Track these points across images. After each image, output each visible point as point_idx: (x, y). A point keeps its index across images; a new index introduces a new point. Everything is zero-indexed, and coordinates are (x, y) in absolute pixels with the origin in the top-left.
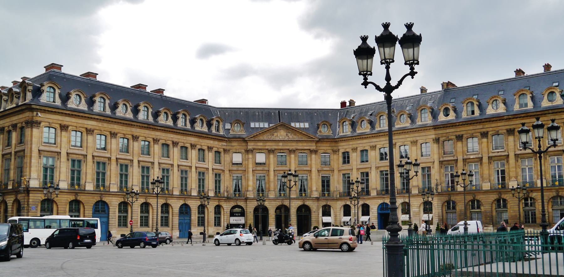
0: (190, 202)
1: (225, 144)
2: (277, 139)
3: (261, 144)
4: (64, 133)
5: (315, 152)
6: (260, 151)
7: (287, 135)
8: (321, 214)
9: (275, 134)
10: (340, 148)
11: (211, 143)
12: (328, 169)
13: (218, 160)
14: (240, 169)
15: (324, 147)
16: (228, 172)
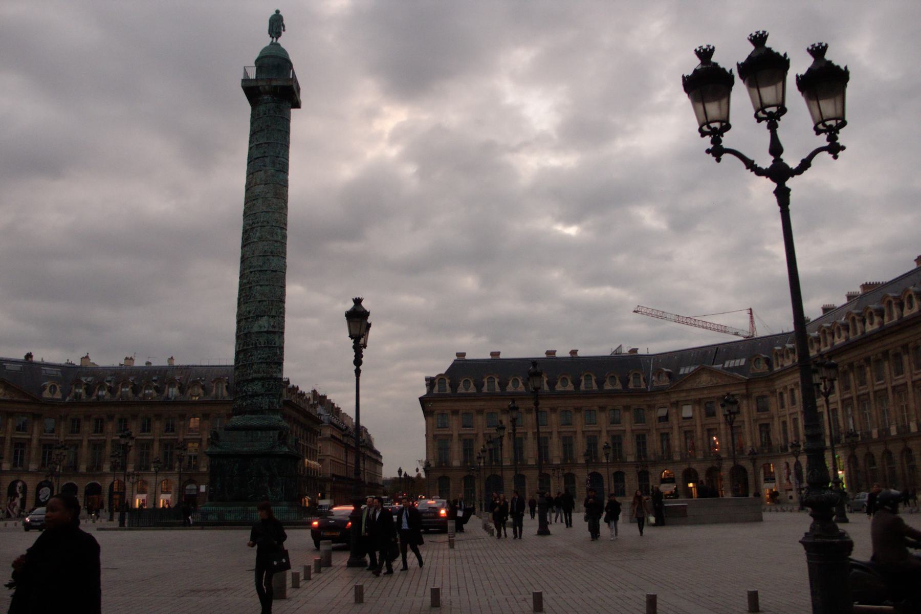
0: (602, 471)
1: (648, 399)
2: (701, 386)
3: (684, 394)
4: (454, 418)
5: (747, 396)
6: (686, 403)
7: (711, 379)
8: (762, 478)
9: (698, 380)
10: (776, 387)
11: (626, 401)
12: (766, 416)
13: (639, 419)
14: (667, 426)
15: (759, 389)
16: (654, 432)
